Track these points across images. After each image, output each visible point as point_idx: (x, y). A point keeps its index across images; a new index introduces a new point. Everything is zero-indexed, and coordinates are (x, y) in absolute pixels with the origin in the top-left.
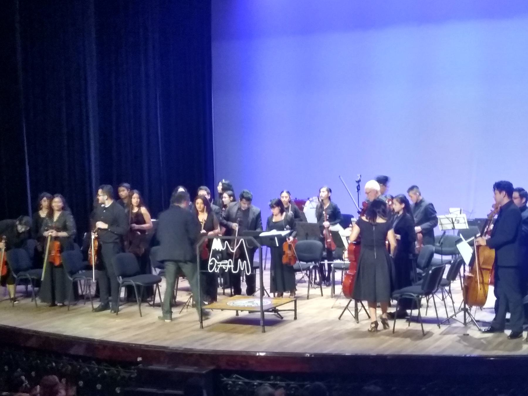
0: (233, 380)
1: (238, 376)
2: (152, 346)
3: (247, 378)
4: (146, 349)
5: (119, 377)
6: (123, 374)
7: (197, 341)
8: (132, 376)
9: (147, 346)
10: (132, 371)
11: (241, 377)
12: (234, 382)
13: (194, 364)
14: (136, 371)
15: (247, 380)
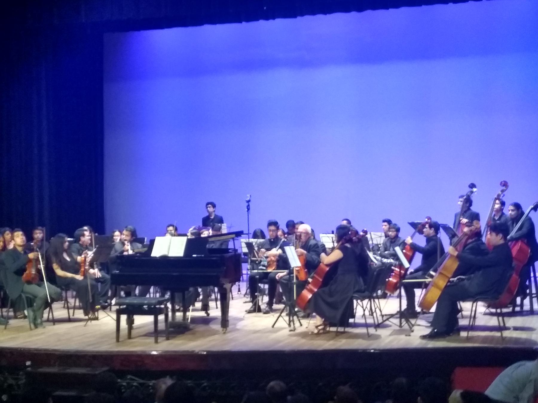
0: (128, 381)
1: (134, 378)
2: (40, 350)
3: (143, 379)
4: (35, 352)
5: (6, 384)
6: (11, 381)
7: (89, 345)
8: (20, 382)
9: (36, 350)
10: (20, 377)
11: (136, 379)
12: (128, 383)
13: (86, 366)
14: (24, 377)
15: (141, 381)
